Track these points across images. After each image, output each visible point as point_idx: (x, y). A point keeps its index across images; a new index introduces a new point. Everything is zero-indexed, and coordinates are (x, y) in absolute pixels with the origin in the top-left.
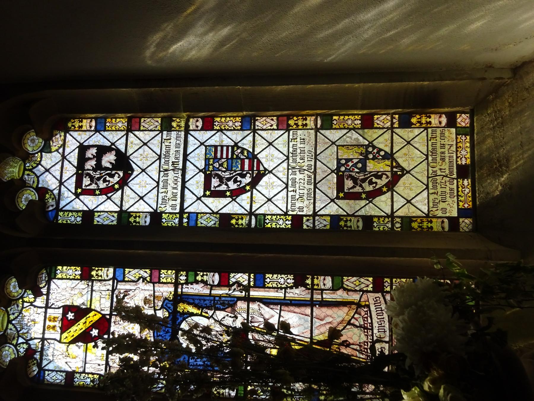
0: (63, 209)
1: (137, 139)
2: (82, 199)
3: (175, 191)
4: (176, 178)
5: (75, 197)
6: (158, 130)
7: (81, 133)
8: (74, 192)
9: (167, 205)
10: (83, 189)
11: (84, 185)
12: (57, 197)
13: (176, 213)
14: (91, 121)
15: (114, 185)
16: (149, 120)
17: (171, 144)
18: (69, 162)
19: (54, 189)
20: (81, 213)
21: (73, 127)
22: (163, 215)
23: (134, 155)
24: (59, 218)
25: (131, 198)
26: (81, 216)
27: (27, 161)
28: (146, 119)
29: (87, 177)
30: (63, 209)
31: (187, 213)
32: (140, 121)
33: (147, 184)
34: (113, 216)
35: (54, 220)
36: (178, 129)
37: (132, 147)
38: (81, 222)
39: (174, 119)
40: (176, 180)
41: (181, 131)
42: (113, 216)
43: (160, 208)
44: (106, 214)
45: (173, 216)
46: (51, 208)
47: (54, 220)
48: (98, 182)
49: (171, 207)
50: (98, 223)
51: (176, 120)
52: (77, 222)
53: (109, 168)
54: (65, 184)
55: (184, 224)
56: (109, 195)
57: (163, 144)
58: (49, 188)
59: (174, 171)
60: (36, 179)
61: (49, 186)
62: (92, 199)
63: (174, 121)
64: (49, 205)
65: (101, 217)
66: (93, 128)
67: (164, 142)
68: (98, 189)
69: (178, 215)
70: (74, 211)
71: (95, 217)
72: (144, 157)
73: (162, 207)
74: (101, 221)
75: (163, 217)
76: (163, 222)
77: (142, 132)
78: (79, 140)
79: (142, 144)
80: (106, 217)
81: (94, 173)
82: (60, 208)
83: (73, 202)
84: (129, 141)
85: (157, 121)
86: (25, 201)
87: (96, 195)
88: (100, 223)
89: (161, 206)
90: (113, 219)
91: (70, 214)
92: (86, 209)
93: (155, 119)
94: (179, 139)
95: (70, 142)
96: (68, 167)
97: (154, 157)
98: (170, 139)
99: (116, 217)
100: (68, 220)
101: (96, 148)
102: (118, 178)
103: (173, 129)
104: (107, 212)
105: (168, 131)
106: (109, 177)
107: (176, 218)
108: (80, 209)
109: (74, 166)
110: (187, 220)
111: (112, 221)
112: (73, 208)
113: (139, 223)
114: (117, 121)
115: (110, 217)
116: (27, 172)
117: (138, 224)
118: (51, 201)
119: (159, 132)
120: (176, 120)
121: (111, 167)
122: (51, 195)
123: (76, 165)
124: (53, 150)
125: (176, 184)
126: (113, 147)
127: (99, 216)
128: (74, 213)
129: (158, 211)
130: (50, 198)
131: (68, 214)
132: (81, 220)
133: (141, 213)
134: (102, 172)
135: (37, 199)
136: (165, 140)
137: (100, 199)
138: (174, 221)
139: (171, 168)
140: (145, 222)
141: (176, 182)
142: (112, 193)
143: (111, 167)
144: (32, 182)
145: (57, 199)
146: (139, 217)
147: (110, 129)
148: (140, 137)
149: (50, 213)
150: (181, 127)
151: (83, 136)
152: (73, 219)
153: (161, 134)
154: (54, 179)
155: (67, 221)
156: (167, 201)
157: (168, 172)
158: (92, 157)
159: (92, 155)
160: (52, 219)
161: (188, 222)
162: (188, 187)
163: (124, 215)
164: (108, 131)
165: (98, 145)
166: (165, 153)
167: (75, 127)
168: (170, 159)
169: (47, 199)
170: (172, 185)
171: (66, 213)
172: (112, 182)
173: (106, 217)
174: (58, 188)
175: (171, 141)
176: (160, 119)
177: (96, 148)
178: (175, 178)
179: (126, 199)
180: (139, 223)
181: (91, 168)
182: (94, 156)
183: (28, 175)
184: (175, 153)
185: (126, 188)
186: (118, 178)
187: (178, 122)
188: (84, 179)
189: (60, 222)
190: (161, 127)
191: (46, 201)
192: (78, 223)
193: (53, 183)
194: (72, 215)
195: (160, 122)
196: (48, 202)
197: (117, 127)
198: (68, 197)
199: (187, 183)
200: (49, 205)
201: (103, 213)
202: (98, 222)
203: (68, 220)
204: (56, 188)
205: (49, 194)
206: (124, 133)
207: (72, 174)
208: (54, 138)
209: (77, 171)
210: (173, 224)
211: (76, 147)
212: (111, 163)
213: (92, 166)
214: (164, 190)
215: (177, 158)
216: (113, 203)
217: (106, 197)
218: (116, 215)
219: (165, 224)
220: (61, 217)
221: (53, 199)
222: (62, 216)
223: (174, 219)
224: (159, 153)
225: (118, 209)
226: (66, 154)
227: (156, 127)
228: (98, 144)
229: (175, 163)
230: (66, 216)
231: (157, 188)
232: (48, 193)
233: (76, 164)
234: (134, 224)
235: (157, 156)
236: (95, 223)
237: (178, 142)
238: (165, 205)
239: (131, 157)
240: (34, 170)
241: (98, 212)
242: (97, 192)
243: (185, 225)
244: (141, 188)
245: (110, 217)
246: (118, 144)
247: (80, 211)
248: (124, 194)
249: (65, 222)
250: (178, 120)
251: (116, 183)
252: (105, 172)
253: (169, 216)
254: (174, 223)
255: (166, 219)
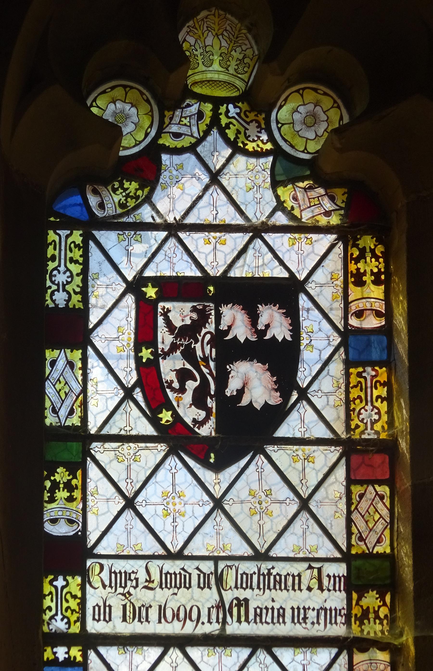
0: (92, 244)
1: (320, 476)
2: (123, 303)
3: (154, 614)
4: (194, 616)
5: (130, 278)
6: (349, 546)
7: (340, 282)
8: (148, 273)
9: (108, 589)
10: (155, 303)
11: (168, 305)
12: (130, 220)
13: (83, 620)
14: (378, 314)
15: (170, 407)
16: (385, 512)
17: (305, 592)
18: (244, 251)
19: (154, 207)
20: (81, 305)
21: (356, 253)
22: (79, 579)
23: (268, 467)
24: (63, 233)
25: (128, 468)
26: (71, 306)
27: (244, 106)
28: (387, 501)
29: (195, 316)
30: (91, 243)
31: (85, 656)
32: (381, 483)
33: (174, 521)
34: (71, 412)
35: (57, 215)
36: (354, 612)
37: (295, 459)
38: (52, 305)
39: (388, 599)
40: (188, 616)
41: (348, 623)
42: (71, 412)
43: (97, 569)
44: (77, 388)
45: (73, 611)
46: (93, 201)
47: (57, 215)
48: (178, 352)
49: (101, 604)
50: (48, 363)
51: (385, 604)
52: (52, 294)
53: (226, 387)
54: (172, 242)
55: (49, 649)
56: (138, 395)
57: (306, 565)
58: (159, 188)
59: (218, 607)
60: (186, 142)
61: (163, 189)
62: (126, 337)
63: (382, 598)
64: (104, 193)
65: (68, 372)
66: (354, 322)
67: (310, 567)
68: (155, 354)
69: (75, 629)
70: (85, 281)
71: (68, 351)
72: (260, 503)
73: (103, 575)
74: (55, 375)
75: (69, 578)
76: (56, 579)
77: (343, 490)
78: (314, 277)
79: (305, 495)
80: (67, 389)
81: (208, 337)
82: (95, 233)
83: (114, 274)
84: (315, 448)
85: (379, 541)
86: (115, 114)
87: (137, 349)
88: (48, 369)
89: (106, 569)
90: (63, 413)
91: (76, 269)
92: (93, 319)
93: (387, 533)
94: (322, 617)
95: (307, 248)
96: (226, 249)
97: (261, 534)
98: (321, 588)
99: (69, 423)
100: (56, 264)
101: (289, 338)
102: (194, 420)
103: (355, 596)
104: (84, 390)
105: (347, 579)
106: (196, 391)
107: (69, 623)
108: (92, 300)
109: (230, 266)
110: (61, 659)
111: (55, 411)
112: (97, 276)
113: (52, 500)
114: (378, 404)
115: (68, 402)
116: (208, 108)
117: (46, 496)
118: (116, 198)
119: (344, 548)
120: (385, 604)
121: (228, 393)
122: (137, 198)
123: (232, 274)
124: (280, 191)
125: (176, 616)
126: (295, 396)
127: (71, 365)
128: (78, 280)
129: (89, 563)
130: (127, 196)
131: (76, 262)
132: (57, 305)
133: (81, 506)
134: (212, 364)
135: (123, 153)
136: (320, 570)
137: (123, 364)
138: (59, 617)
139: (228, 596)
140: (54, 521)
141: (182, 615)
142: (143, 404)
143: (228, 393)
144: (174, 129)
145: (124, 220)
146: (70, 499)
147: (353, 380)
148: (326, 484)
149: (78, 199)
150: (362, 624)
151: (328, 292)
152: (61, 278)
153: (338, 555)
154: (189, 205)
155: (53, 258)
156: (120, 590)
157: (214, 587)
158: (260, 327)
159: (268, 326)
160: (58, 207)
161: (55, 662)
162: (167, 658)
163: (76, 446)
164: (347, 375)
165: (299, 345)
166: (274, 572)
167: (357, 260)
168: (256, 591)
169: (121, 186)
170: (173, 605)
171: (77, 254)
172: (178, 400)
173: (67, 389)
174: (158, 220)
175: (316, 591)
176: (388, 551)
177: (289, 338)
178: (195, 610)
179: (126, 452)
180: (52, 500)
181: (223, 327)
182: (264, 332)
183: (200, 115)
184: (277, 606)
185: (162, 448)
186: (194, 420)
187: (376, 613)
188: (189, 305)
189: (52, 236)
190: (363, 556)
191: (117, 184)
192: (48, 297)
193: (173, 200)
194: (72, 276)
195: (379, 549)
196: (115, 190)
197: (358, 405)
198: (129, 254)
199: (181, 655)
200: (104, 193)
201: (80, 378)
202: (53, 363)
203: (56, 264)
204: (158, 212)
205: (139, 193)
206: (340, 428)
207: (203, 263)
208: (321, 191)
209: (214, 280)
210: (46, 617)
211: (294, 270)
212: (241, 392)
213: (230, 327)
214: (156, 576)
215: (258, 615)
216: (111, 408)
217: (132, 382)
218: (75, 420)
219: (47, 588)
220: (67, 237)
221: (122, 206)
222: (70, 240)
223: (64, 617)
224: (275, 552)
225: (93, 429)
226: (270, 237)
227: (361, 539)
228: (304, 342)
229: (242, 610)
230: (69, 255)
231: (161, 552)
232: (141, 188)
233: (238, 275)
234: (48, 484)
235: (266, 546)
236: (50, 354)
237: (312, 615)
238: (107, 583)
239: (261, 459)
240: (215, 131)
241: (84, 359)
242: (146, 354)
243: (48, 654)
244: (159, 500)
245: (68, 402)
246: (302, 411)
247: (85, 300)
248: (143, 445)
249: (50, 251)
250: (383, 612)
251: (176, 415)
252: (211, 374)
253: (74, 597)
254: (52, 617)
255: (63, 588)
